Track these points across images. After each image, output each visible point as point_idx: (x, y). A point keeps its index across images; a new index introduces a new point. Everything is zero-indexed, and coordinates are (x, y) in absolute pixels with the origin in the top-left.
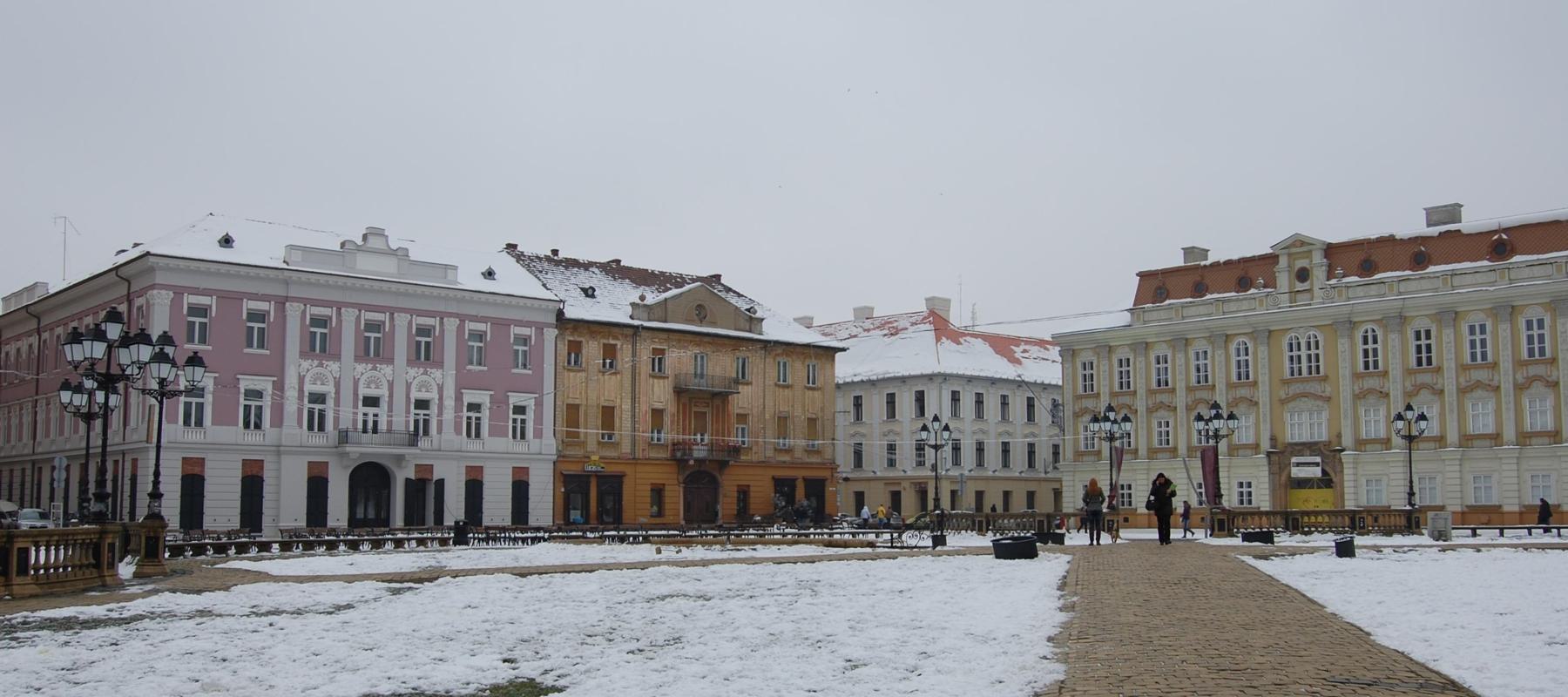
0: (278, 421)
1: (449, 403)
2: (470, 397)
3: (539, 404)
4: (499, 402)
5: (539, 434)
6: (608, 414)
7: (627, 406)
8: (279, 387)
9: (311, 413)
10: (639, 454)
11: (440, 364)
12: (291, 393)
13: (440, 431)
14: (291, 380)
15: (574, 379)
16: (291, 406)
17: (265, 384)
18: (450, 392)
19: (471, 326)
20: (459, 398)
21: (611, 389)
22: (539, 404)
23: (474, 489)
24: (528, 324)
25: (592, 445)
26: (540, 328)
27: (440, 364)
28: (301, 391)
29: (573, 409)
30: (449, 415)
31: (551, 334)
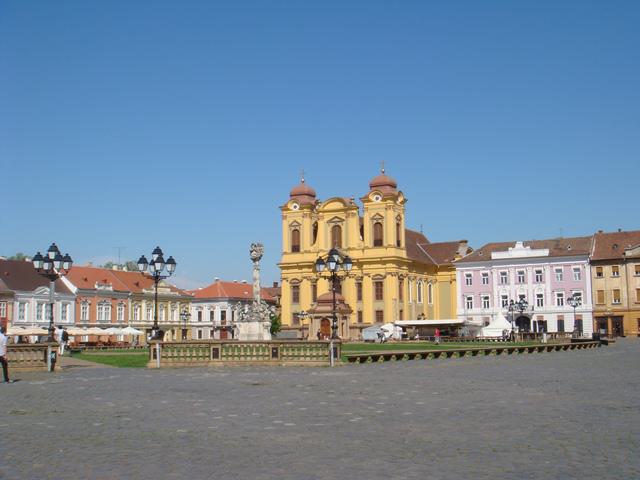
0: (493, 305)
3: (585, 292)
5: (586, 302)
6: (617, 291)
7: (625, 289)
8: (493, 296)
10: (631, 307)
11: (544, 282)
14: (496, 293)
15: (600, 283)
16: (496, 301)
18: (549, 291)
19: (555, 268)
21: (616, 283)
23: (561, 323)
25: (609, 305)
27: (544, 282)
29: (601, 292)
30: (549, 299)
31: (588, 268)
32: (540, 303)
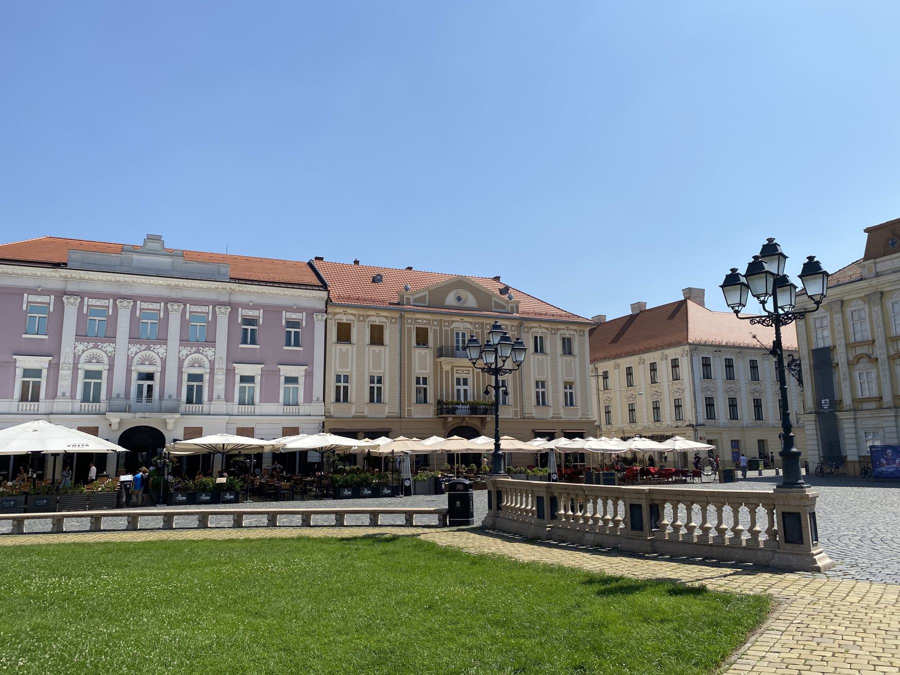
0: (53, 395)
1: (220, 377)
2: (244, 369)
3: (309, 375)
4: (270, 375)
8: (54, 368)
9: (86, 386)
12: (65, 373)
13: (211, 399)
16: (64, 384)
17: (40, 363)
18: (221, 365)
20: (230, 372)
22: (309, 375)
24: (299, 310)
26: (311, 313)
28: (75, 369)
30: (220, 388)
32: (194, 397)
